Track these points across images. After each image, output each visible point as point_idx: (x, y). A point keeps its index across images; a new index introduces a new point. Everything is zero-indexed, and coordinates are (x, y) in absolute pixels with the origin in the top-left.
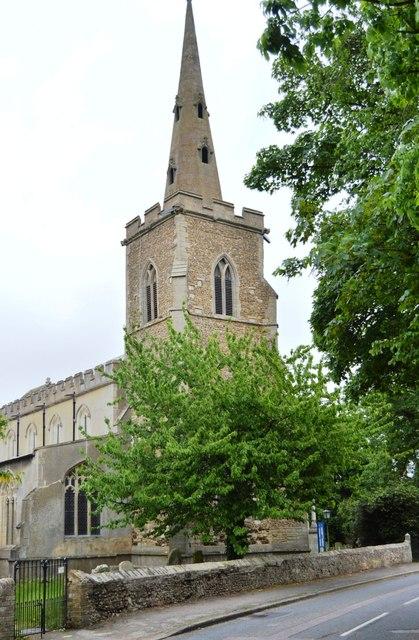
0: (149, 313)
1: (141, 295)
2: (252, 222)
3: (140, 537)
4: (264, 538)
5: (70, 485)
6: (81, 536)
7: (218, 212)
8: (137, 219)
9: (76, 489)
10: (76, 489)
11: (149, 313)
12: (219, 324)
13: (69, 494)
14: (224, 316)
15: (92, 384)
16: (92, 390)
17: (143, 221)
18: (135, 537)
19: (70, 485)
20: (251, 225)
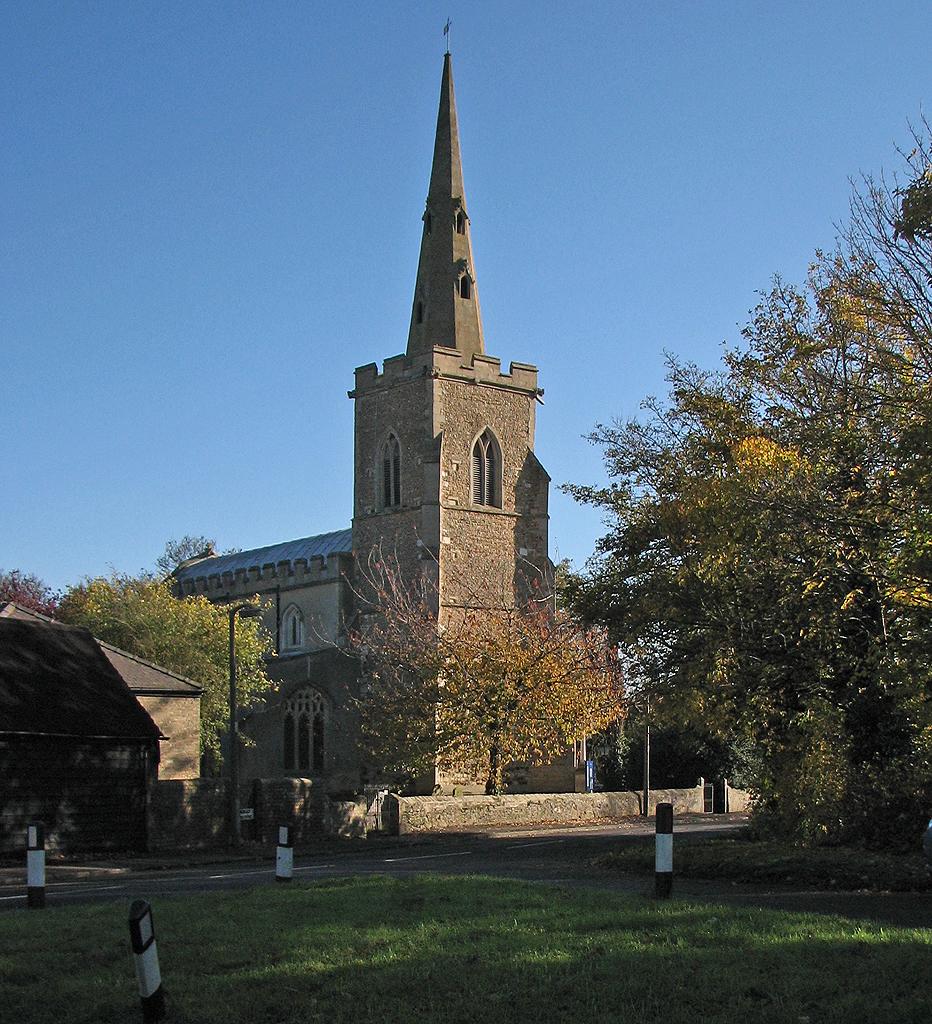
0: (388, 495)
1: (376, 471)
2: (522, 381)
3: (371, 774)
4: (522, 778)
5: (290, 709)
6: (302, 771)
7: (482, 371)
8: (373, 367)
9: (296, 716)
10: (296, 716)
11: (388, 495)
12: (478, 518)
13: (289, 719)
14: (486, 508)
15: (306, 578)
16: (306, 586)
17: (381, 371)
18: (365, 773)
19: (290, 709)
20: (521, 384)
